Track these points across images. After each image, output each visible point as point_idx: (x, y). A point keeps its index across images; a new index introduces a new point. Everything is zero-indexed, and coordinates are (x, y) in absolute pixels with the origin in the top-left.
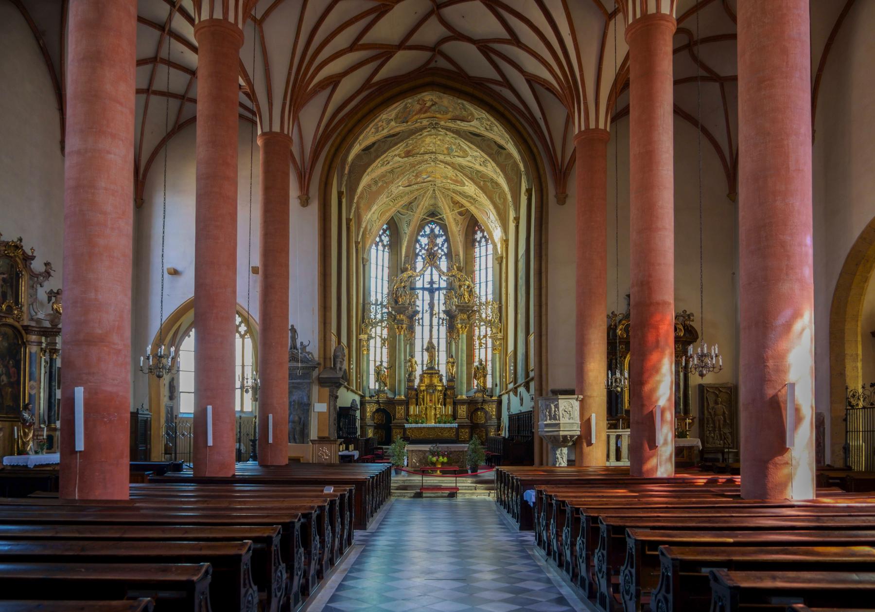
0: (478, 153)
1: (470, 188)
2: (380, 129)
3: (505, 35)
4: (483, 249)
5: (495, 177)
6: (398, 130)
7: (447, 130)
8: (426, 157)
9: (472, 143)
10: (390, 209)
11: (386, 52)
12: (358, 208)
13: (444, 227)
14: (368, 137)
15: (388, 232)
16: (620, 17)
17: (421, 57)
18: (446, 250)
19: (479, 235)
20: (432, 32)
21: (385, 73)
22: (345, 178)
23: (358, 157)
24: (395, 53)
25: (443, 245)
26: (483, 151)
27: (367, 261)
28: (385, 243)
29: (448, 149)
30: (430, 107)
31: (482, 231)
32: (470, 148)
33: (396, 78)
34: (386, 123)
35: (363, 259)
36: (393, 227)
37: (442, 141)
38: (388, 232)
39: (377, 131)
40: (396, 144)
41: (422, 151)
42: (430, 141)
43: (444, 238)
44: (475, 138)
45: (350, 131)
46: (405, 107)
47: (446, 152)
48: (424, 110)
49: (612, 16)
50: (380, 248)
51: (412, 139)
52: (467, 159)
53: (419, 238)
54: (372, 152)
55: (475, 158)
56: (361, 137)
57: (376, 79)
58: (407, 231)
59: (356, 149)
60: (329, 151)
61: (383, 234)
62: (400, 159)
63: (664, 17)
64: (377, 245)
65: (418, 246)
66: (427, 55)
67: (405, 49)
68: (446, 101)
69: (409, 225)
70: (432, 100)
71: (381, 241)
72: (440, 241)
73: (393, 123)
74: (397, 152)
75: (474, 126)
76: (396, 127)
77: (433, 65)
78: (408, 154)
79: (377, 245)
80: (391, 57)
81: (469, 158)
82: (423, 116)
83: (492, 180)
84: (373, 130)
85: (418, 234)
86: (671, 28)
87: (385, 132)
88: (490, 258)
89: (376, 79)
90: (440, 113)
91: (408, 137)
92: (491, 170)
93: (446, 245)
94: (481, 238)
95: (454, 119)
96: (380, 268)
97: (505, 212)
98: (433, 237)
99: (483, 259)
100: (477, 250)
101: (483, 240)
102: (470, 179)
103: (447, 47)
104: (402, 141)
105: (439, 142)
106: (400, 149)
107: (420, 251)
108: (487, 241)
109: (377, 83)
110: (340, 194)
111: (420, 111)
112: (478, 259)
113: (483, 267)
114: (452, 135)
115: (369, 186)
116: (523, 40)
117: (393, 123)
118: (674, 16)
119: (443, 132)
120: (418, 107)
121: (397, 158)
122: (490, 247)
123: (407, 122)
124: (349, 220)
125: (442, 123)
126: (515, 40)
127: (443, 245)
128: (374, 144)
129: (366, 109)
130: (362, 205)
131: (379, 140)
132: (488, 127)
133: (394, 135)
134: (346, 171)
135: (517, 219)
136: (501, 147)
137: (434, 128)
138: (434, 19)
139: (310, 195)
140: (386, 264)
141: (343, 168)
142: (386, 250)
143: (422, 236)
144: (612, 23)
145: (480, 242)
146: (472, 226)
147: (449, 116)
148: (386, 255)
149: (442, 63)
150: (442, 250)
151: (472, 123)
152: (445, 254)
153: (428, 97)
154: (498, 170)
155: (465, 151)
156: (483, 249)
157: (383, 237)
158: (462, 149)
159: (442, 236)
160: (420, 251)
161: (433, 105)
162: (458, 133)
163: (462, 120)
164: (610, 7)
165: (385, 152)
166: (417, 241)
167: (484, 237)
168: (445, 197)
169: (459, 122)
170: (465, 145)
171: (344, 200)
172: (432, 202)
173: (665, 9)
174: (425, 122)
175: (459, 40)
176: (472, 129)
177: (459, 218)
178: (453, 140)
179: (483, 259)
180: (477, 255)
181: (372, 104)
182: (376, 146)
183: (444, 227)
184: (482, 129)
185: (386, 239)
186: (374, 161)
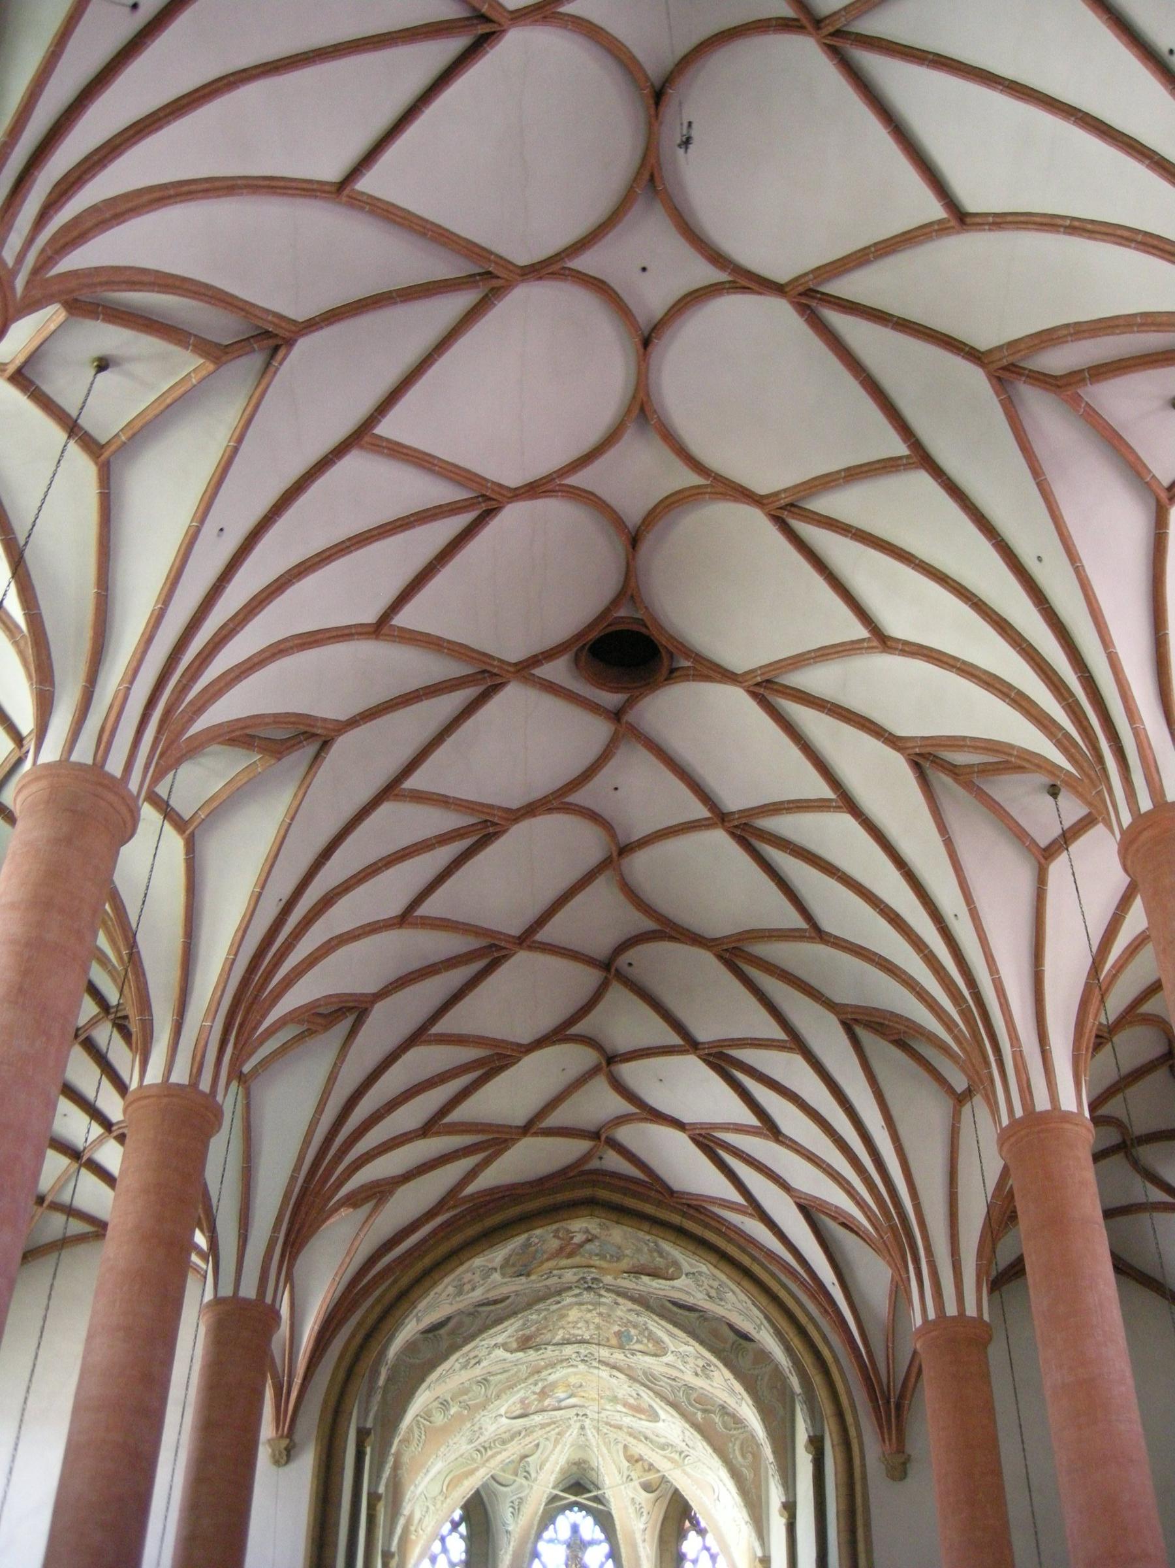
0: (692, 1348)
1: (671, 1427)
2: (467, 1287)
3: (752, 1120)
5: (731, 1402)
6: (505, 1290)
7: (619, 1294)
8: (569, 1350)
9: (675, 1324)
10: (472, 1472)
11: (496, 1139)
12: (396, 1467)
13: (605, 1521)
14: (439, 1303)
16: (978, 1099)
17: (568, 1151)
19: (691, 1544)
20: (598, 1103)
21: (490, 1178)
22: (377, 1398)
23: (411, 1347)
24: (514, 1141)
26: (702, 1343)
29: (618, 1334)
30: (581, 1245)
31: (702, 1532)
32: (671, 1335)
33: (512, 1187)
34: (485, 1273)
36: (478, 1517)
37: (606, 1317)
38: (463, 1529)
39: (460, 1292)
40: (499, 1321)
41: (558, 1338)
42: (577, 1316)
44: (685, 1317)
45: (403, 1295)
46: (527, 1245)
47: (614, 1341)
48: (568, 1250)
49: (961, 1099)
51: (538, 1312)
52: (665, 1359)
53: (542, 1546)
54: (445, 1340)
55: (683, 1357)
56: (422, 1305)
57: (470, 1189)
58: (513, 1526)
59: (409, 1330)
60: (353, 1336)
62: (507, 1355)
63: (1066, 1117)
66: (584, 1145)
67: (535, 1134)
68: (619, 1235)
69: (517, 1511)
70: (587, 1231)
73: (496, 1277)
74: (500, 1339)
75: (683, 1288)
76: (501, 1285)
77: (594, 1164)
78: (525, 1344)
80: (507, 1148)
81: (669, 1358)
82: (564, 1262)
83: (724, 1410)
84: (451, 1289)
85: (539, 1536)
86: (1085, 1138)
87: (478, 1295)
89: (470, 1189)
90: (602, 1257)
91: (529, 1306)
92: (723, 1387)
95: (638, 1271)
98: (576, 1546)
102: (674, 1405)
103: (625, 1135)
104: (515, 1313)
105: (597, 1320)
106: (508, 1331)
108: (713, 1558)
109: (472, 1197)
110: (363, 1435)
111: (559, 1253)
114: (630, 1305)
115: (427, 1415)
116: (786, 1128)
117: (496, 1277)
118: (1087, 1114)
119: (608, 1298)
120: (555, 1244)
121: (500, 1353)
123: (528, 1275)
124: (374, 1498)
125: (608, 1279)
126: (770, 1129)
128: (449, 1319)
129: (444, 1249)
130: (405, 1459)
131: (460, 1312)
132: (713, 1293)
133: (496, 1302)
134: (381, 1381)
135: (790, 1508)
136: (746, 1337)
137: (589, 1289)
138: (600, 1087)
139: (297, 1438)
141: (375, 1373)
143: (551, 1541)
144: (966, 1109)
145: (695, 1562)
146: (678, 1517)
147: (625, 1264)
149: (613, 1161)
151: (676, 1283)
153: (580, 1226)
154: (738, 1387)
155: (658, 1342)
158: (651, 1337)
161: (588, 1241)
162: (644, 1302)
163: (654, 1274)
164: (960, 1083)
165: (473, 1337)
168: (608, 1445)
169: (645, 1279)
170: (659, 1328)
171: (368, 1450)
172: (576, 1457)
173: (1068, 1101)
174: (569, 1276)
175: (651, 1121)
176: (677, 1296)
177: (644, 1497)
178: (632, 1317)
181: (456, 1240)
182: (451, 1325)
183: (605, 1521)
184: (700, 1296)
186: (445, 1357)
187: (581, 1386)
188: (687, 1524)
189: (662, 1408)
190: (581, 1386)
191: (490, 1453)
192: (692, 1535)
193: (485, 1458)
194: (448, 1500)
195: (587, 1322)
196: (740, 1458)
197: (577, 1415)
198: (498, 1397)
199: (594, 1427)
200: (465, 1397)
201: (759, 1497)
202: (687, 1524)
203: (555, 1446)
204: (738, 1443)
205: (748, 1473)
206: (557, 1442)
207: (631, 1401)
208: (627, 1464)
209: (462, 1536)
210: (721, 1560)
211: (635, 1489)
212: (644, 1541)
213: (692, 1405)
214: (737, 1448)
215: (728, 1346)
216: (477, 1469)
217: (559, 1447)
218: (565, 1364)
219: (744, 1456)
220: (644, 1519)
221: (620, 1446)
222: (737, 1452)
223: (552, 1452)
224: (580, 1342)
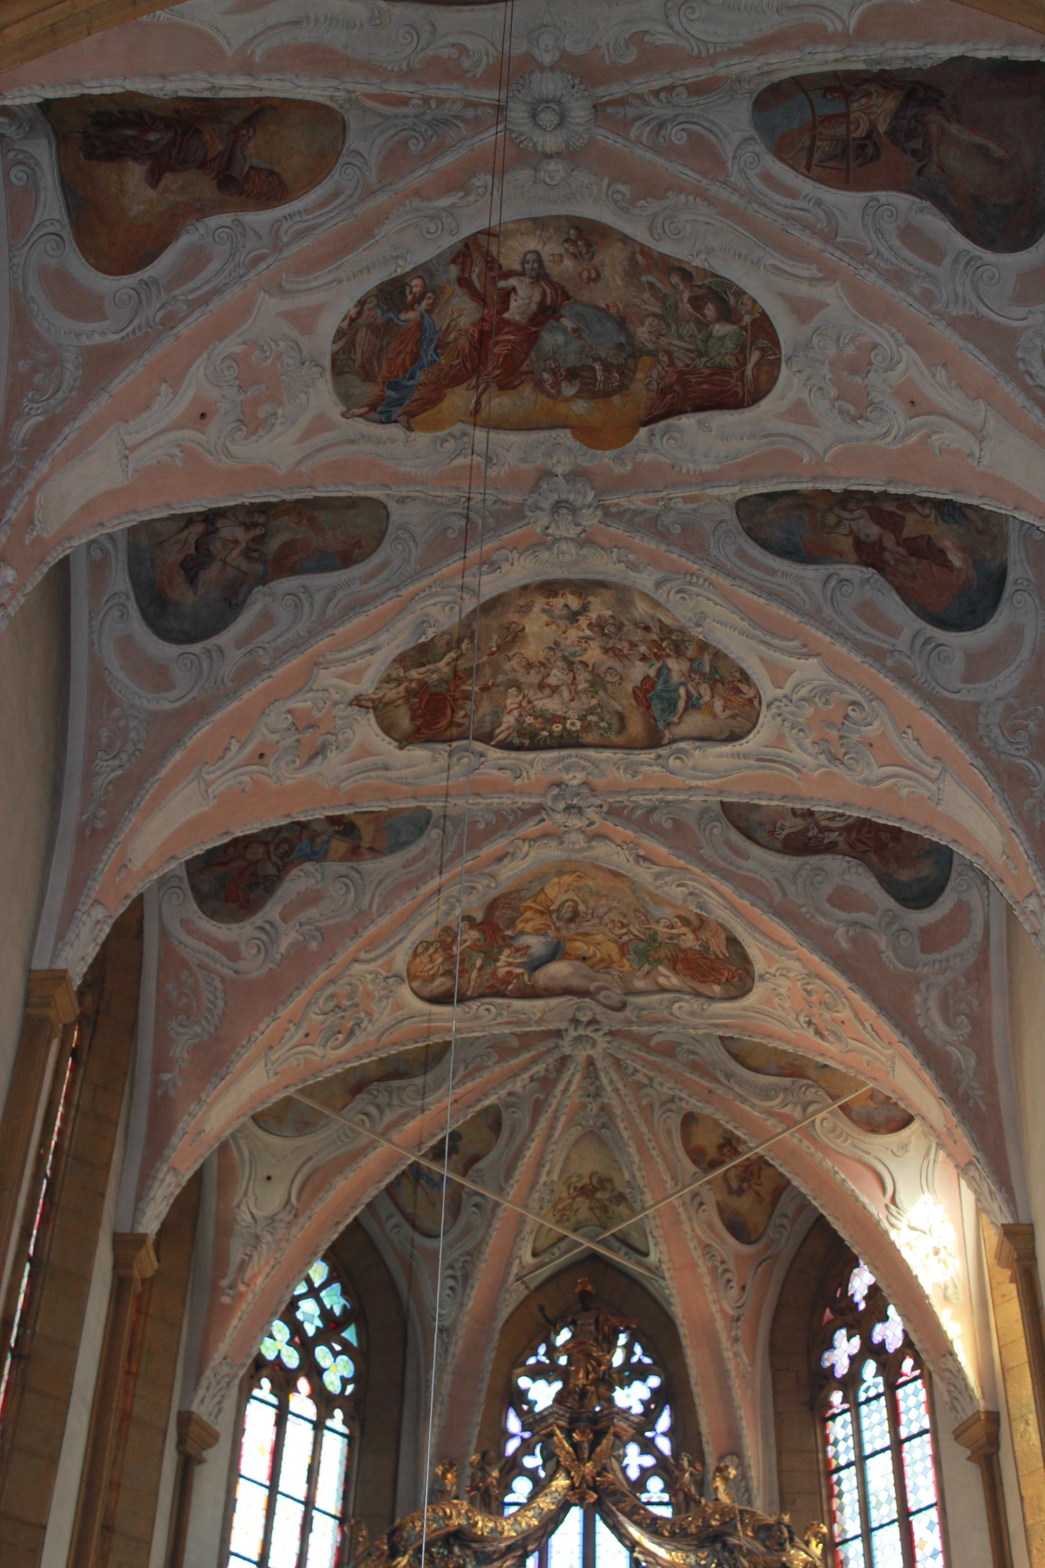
4: (874, 1417)
15: (350, 1334)
18: (664, 1445)
25: (649, 1417)
27: (211, 1438)
28: (332, 1382)
29: (644, 692)
35: (186, 1419)
38: (350, 1334)
43: (654, 1381)
50: (301, 1402)
52: (752, 743)
53: (524, 1382)
61: (324, 1336)
64: (284, 1382)
65: (513, 1424)
71: (313, 1371)
72: (631, 1397)
79: (284, 1382)
88: (919, 1455)
93: (664, 1422)
94: (856, 1362)
96: (289, 1515)
97: (990, 1087)
99: (880, 1470)
100: (839, 1429)
101: (870, 1367)
102: (786, 914)
107: (526, 1448)
112: (848, 1479)
113: (884, 1510)
122: (913, 1398)
127: (649, 1417)
140: (330, 1495)
142: (337, 1420)
143: (537, 1373)
145: (851, 1382)
148: (335, 1449)
150: (648, 1447)
152: (663, 1467)
156: (874, 1417)
157: (322, 1354)
159: (640, 1373)
160: (526, 1448)
166: (518, 1399)
167: (872, 1350)
179: (880, 1470)
180: (843, 1452)
185: (337, 1370)
187: (575, 915)
188: (828, 1314)
189: (753, 926)
190: (575, 915)
191: (389, 1116)
192: (841, 1335)
193: (380, 1128)
194: (301, 1220)
195: (570, 664)
196: (941, 1027)
197: (575, 1022)
198: (385, 906)
199: (617, 1063)
200: (313, 912)
201: (995, 1107)
202: (828, 1314)
203: (534, 1122)
204: (934, 994)
205: (965, 1060)
206: (538, 1107)
207: (689, 941)
208: (692, 1168)
209: (347, 1349)
210: (908, 1364)
211: (711, 1227)
212: (736, 1340)
213: (824, 915)
214: (933, 1003)
215: (902, 642)
216: (362, 1152)
217: (543, 1123)
218: (531, 828)
219: (948, 1022)
220: (734, 1292)
221: (675, 1122)
222: (935, 1015)
223: (528, 1138)
224: (568, 741)
